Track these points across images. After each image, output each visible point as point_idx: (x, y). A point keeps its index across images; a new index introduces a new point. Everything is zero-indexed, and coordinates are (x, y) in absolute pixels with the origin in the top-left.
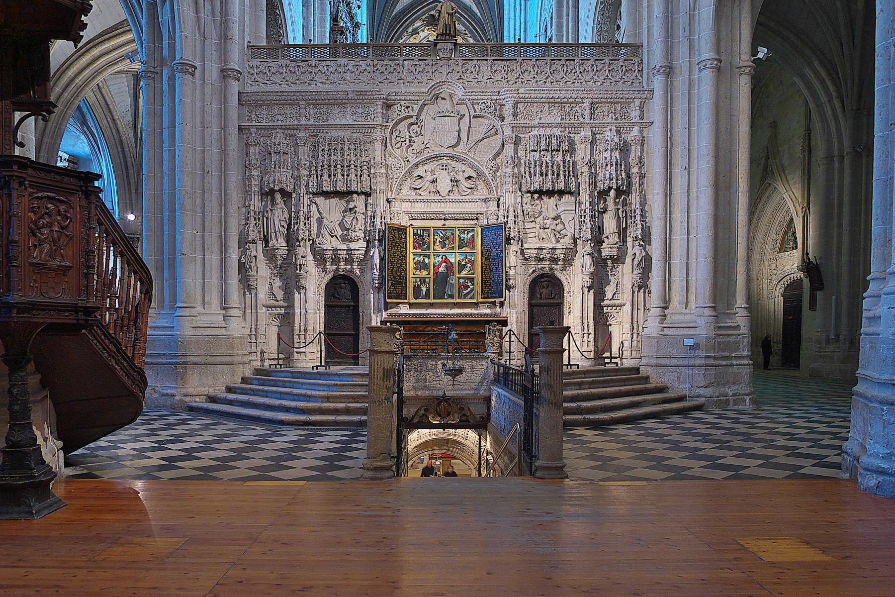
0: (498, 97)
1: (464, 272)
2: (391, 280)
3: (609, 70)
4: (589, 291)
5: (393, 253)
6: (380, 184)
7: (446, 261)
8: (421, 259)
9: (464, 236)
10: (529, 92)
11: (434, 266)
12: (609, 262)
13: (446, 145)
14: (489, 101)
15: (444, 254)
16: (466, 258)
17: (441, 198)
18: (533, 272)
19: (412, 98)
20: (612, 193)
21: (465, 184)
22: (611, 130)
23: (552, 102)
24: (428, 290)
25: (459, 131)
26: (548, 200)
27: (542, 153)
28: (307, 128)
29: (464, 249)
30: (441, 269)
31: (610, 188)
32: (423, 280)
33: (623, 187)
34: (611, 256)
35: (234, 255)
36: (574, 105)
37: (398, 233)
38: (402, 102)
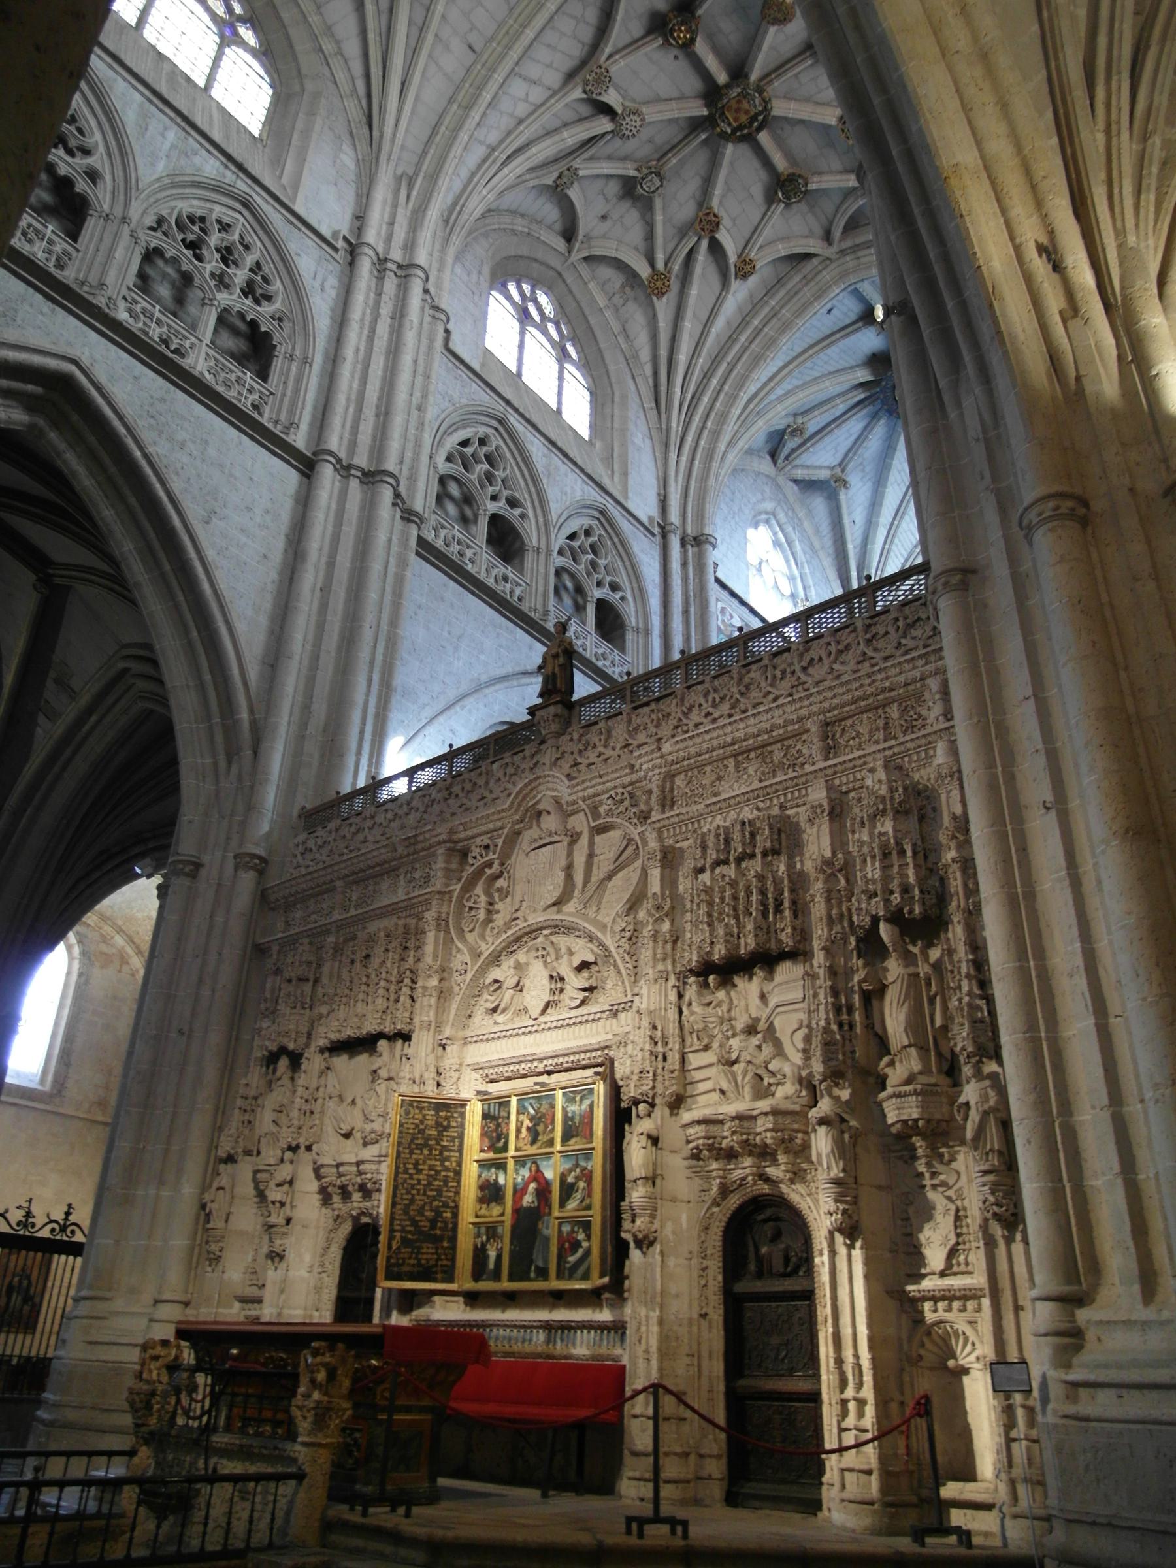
0: (634, 777)
1: (572, 1205)
2: (403, 1230)
3: (869, 641)
4: (851, 1247)
5: (416, 1164)
6: (425, 1011)
7: (537, 1176)
8: (491, 1174)
9: (573, 1108)
10: (681, 746)
11: (515, 1191)
12: (918, 1142)
13: (543, 904)
14: (620, 790)
15: (535, 1160)
16: (577, 1165)
17: (532, 1022)
18: (725, 1191)
19: (491, 826)
20: (885, 931)
21: (576, 982)
22: (872, 770)
23: (741, 755)
24: (499, 1257)
25: (569, 869)
26: (747, 985)
27: (718, 870)
28: (340, 926)
29: (573, 1141)
30: (528, 1199)
31: (875, 920)
32: (492, 1231)
33: (911, 912)
34: (905, 1122)
35: (188, 1190)
36: (791, 742)
37: (437, 1114)
38: (478, 840)
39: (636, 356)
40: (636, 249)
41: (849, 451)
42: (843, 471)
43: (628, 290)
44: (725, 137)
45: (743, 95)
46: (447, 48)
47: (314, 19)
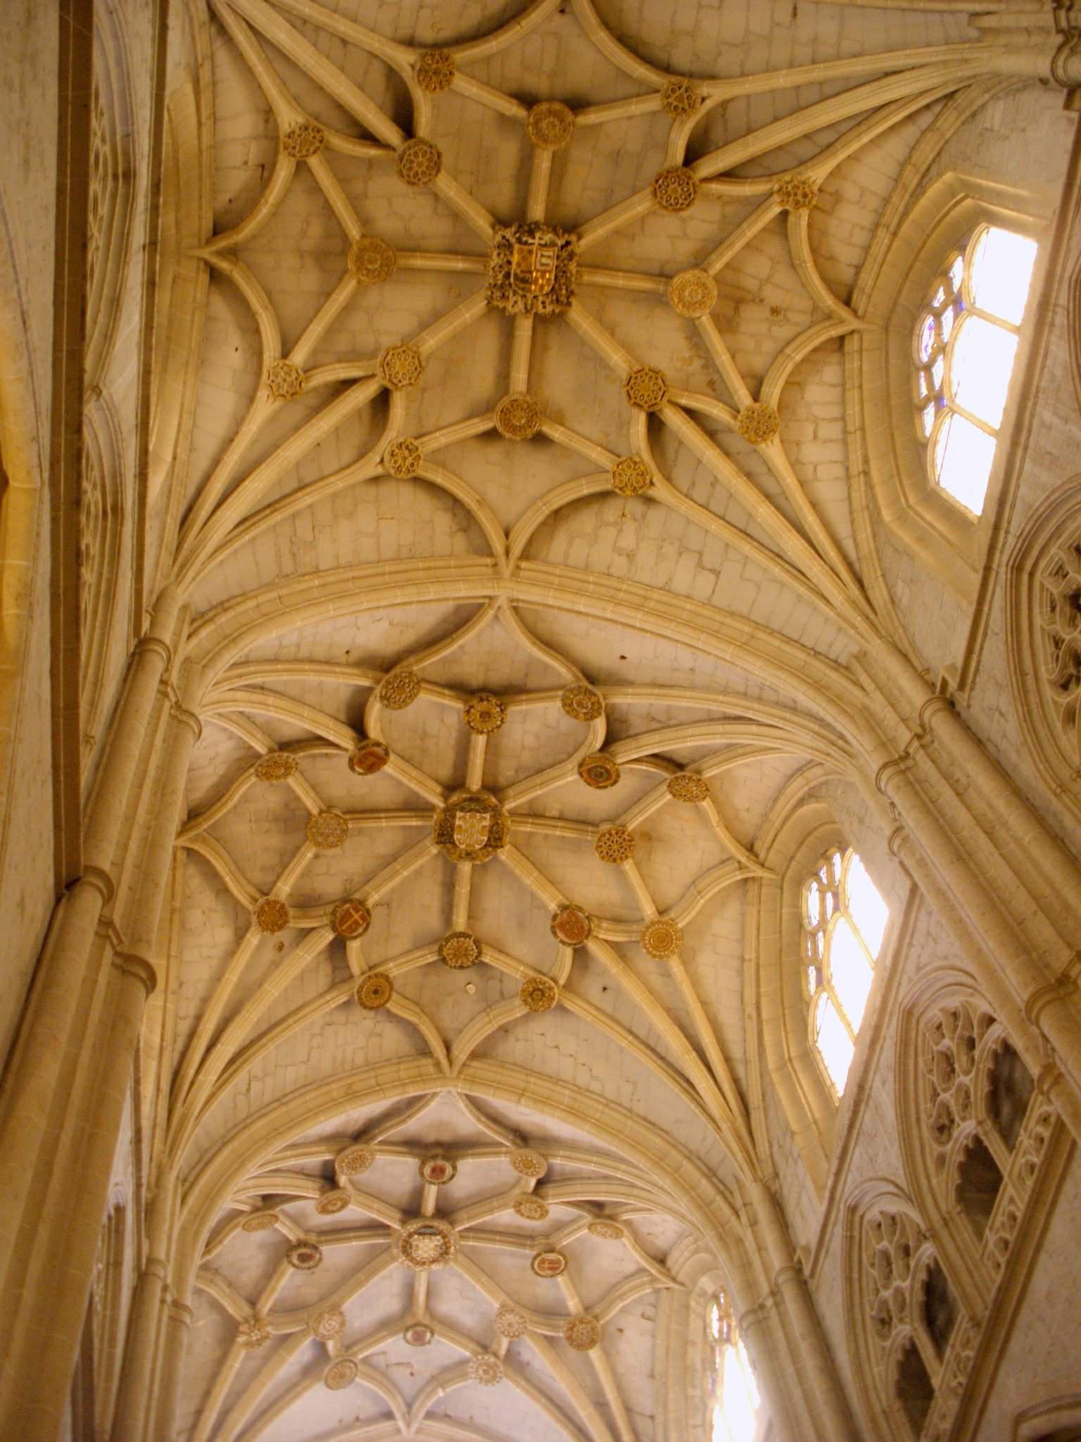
46: (815, 40)
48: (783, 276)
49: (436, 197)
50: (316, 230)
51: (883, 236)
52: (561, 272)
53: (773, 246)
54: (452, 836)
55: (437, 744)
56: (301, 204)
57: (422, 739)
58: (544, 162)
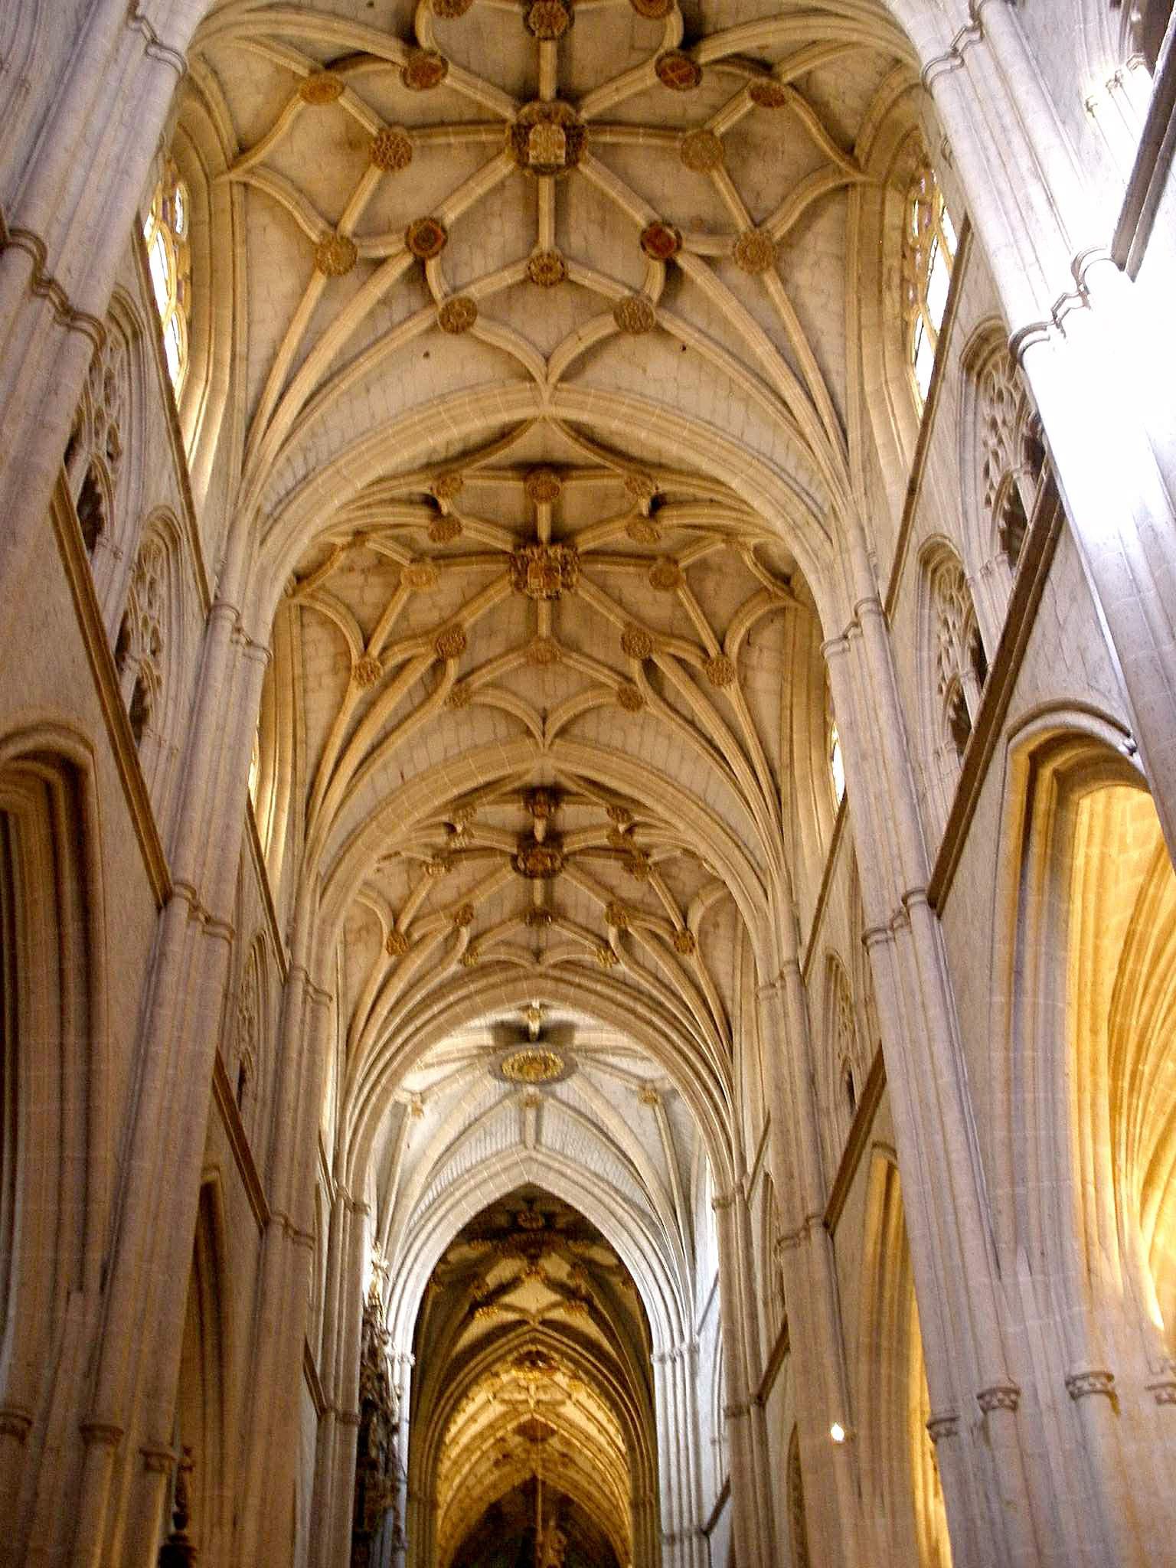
39: (345, 995)
40: (390, 904)
41: (436, 1084)
42: (423, 1101)
43: (364, 933)
44: (516, 869)
45: (552, 857)
47: (300, 704)
48: (352, 596)
49: (620, 602)
50: (710, 585)
51: (298, 671)
52: (522, 573)
53: (366, 612)
54: (568, 137)
55: (588, 212)
56: (723, 609)
57: (604, 220)
58: (544, 629)
